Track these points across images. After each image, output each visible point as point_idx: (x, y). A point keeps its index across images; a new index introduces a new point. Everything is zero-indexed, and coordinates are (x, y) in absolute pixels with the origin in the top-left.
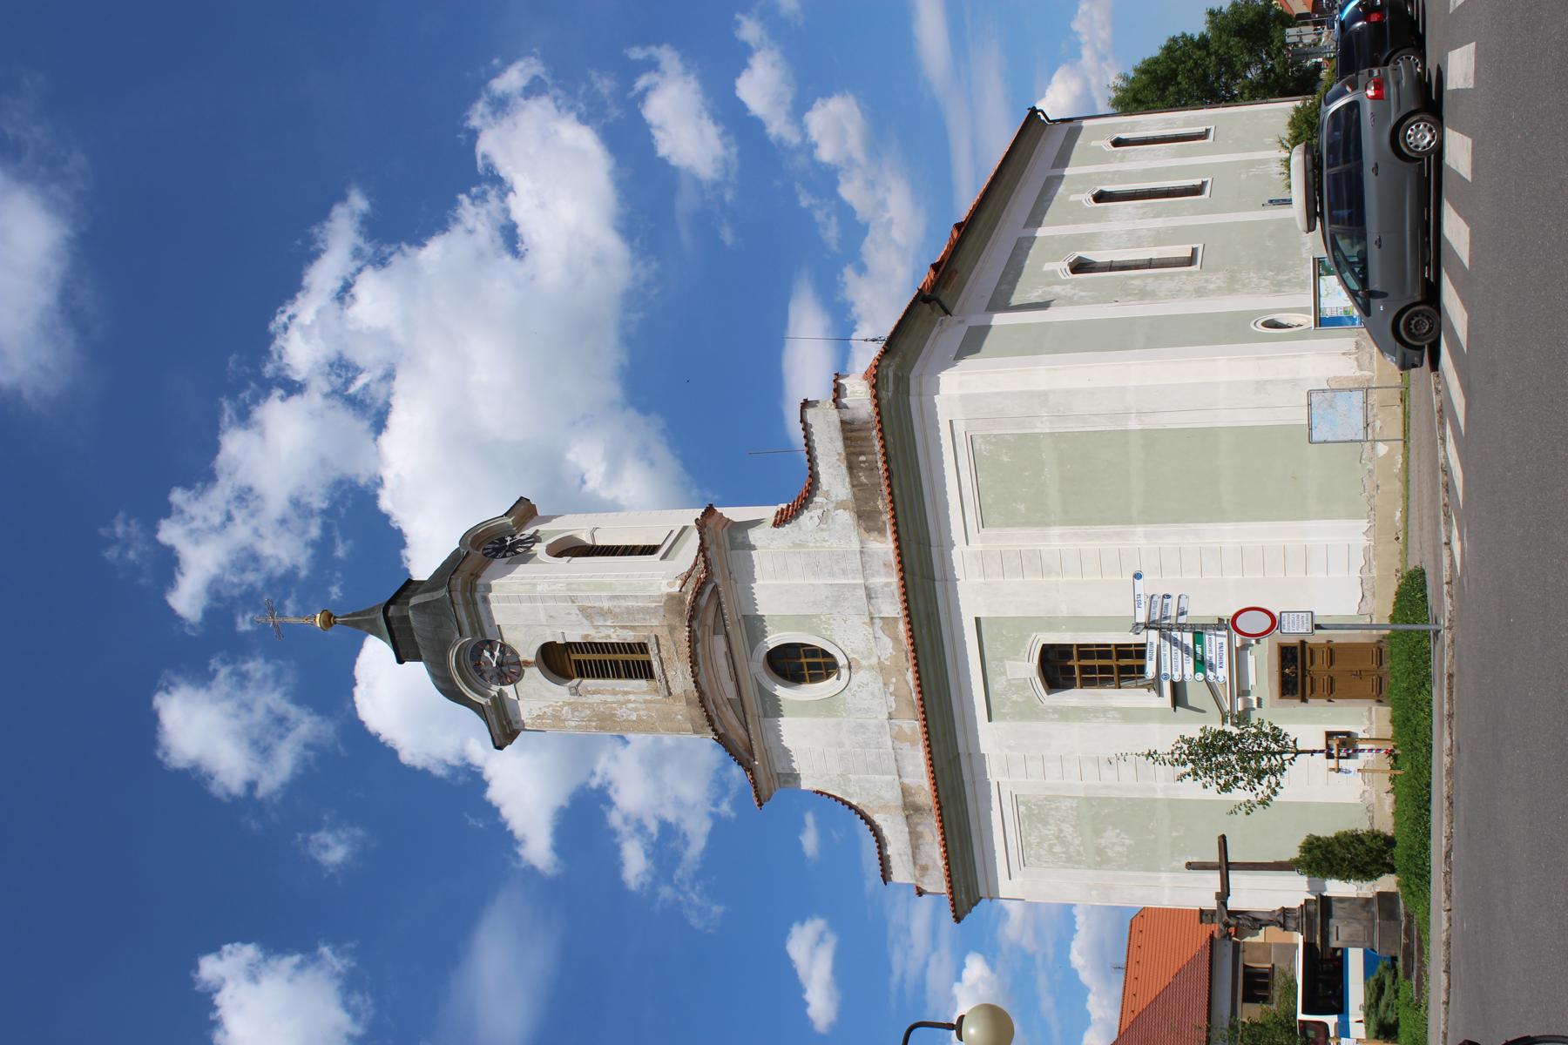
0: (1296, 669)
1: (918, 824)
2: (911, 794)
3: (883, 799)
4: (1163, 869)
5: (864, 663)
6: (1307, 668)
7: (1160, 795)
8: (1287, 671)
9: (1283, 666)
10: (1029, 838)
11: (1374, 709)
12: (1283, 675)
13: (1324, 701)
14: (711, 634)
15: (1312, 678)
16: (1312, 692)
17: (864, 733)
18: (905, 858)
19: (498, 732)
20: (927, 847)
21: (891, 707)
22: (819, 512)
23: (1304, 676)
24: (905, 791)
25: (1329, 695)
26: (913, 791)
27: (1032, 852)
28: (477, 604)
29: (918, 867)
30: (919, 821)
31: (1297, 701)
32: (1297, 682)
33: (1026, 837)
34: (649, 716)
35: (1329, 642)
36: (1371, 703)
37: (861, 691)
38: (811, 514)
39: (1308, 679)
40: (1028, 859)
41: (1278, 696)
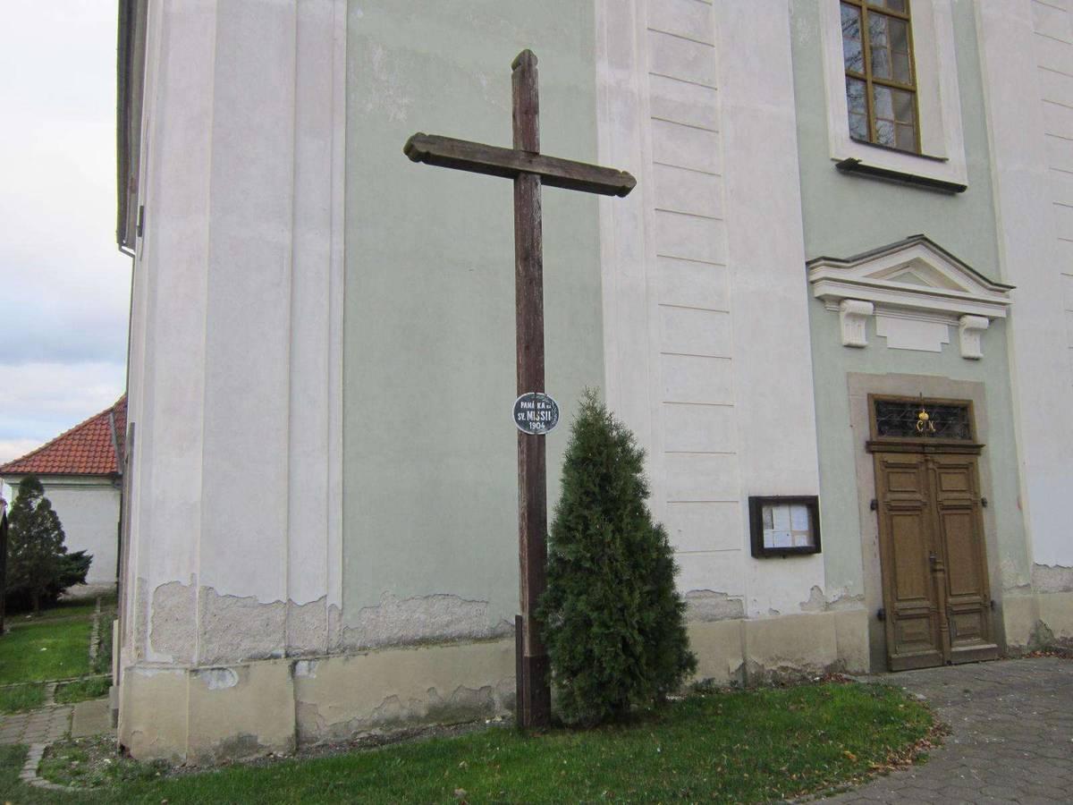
0: (932, 435)
4: (360, 14)
6: (937, 458)
7: (605, 72)
8: (924, 416)
9: (930, 406)
11: (860, 606)
12: (917, 405)
13: (870, 495)
15: (915, 467)
16: (888, 465)
23: (922, 449)
25: (888, 504)
31: (865, 431)
32: (905, 434)
35: (984, 503)
36: (875, 600)
39: (914, 459)
41: (872, 392)
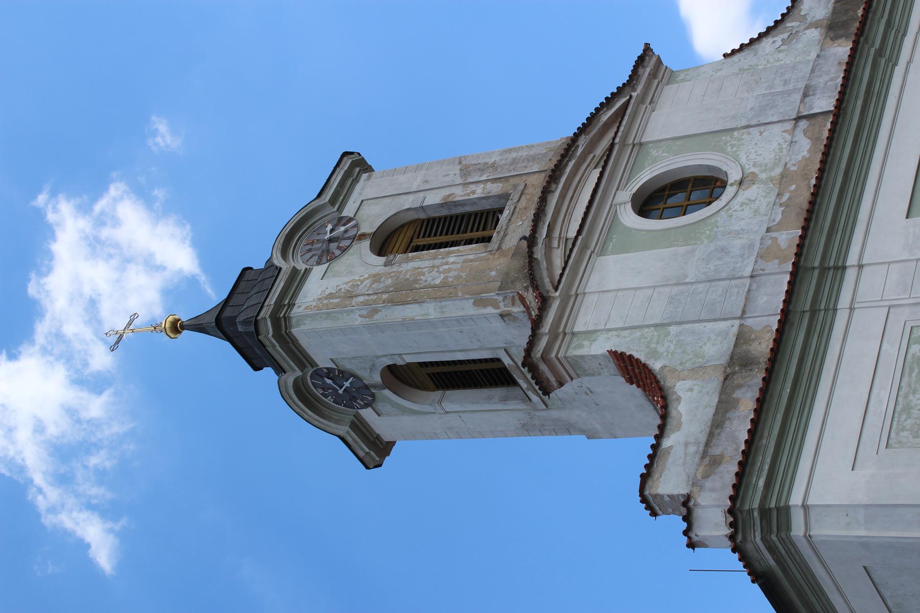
1: (739, 386)
2: (748, 341)
3: (703, 357)
5: (763, 176)
10: (911, 397)
14: (592, 165)
17: (719, 259)
18: (692, 449)
19: (273, 303)
20: (735, 422)
21: (774, 220)
22: (785, 36)
24: (742, 337)
26: (753, 336)
27: (909, 422)
28: (358, 182)
29: (707, 460)
30: (742, 382)
33: (906, 397)
34: (458, 277)
37: (743, 210)
38: (775, 39)
40: (897, 434)
